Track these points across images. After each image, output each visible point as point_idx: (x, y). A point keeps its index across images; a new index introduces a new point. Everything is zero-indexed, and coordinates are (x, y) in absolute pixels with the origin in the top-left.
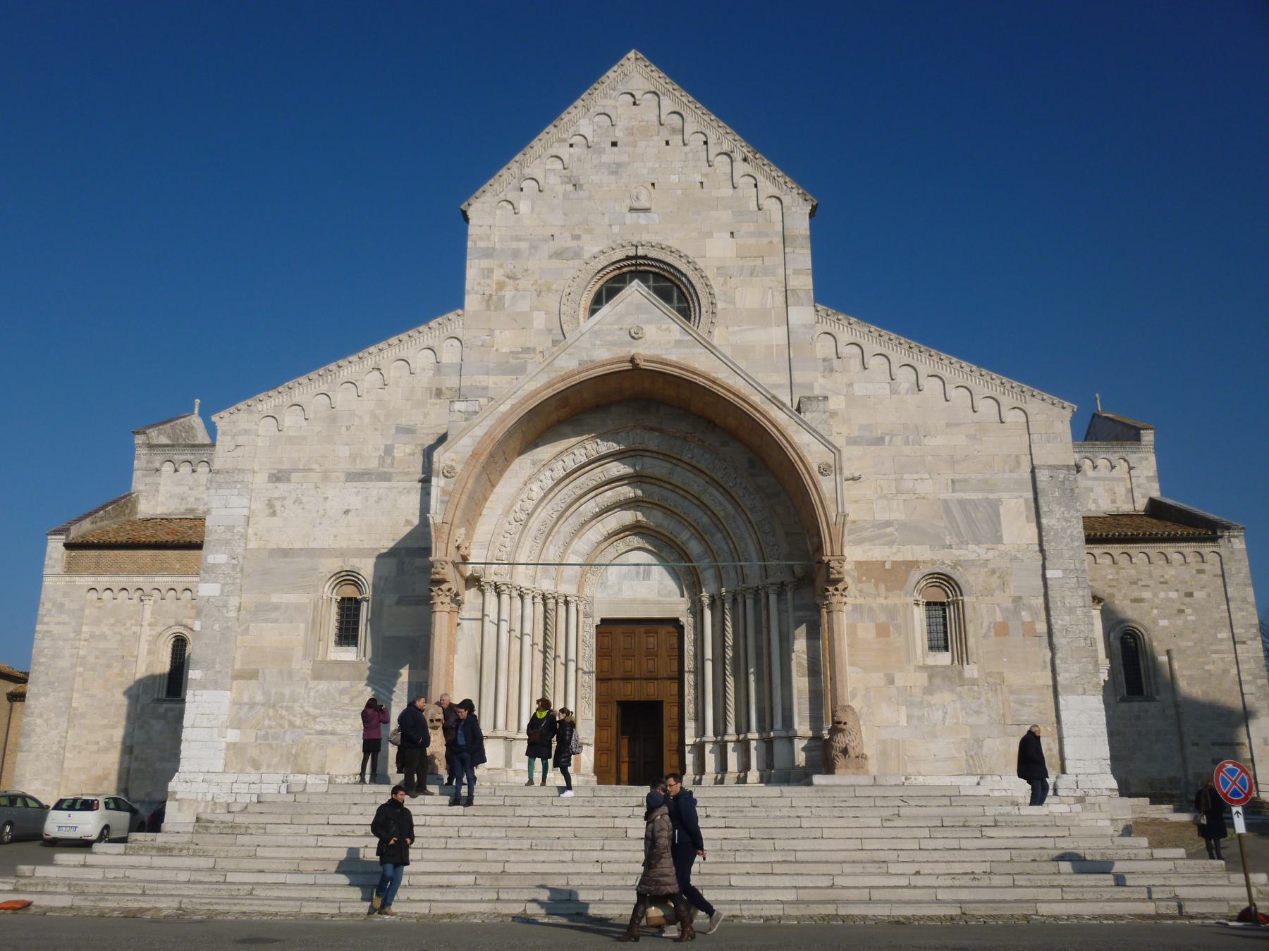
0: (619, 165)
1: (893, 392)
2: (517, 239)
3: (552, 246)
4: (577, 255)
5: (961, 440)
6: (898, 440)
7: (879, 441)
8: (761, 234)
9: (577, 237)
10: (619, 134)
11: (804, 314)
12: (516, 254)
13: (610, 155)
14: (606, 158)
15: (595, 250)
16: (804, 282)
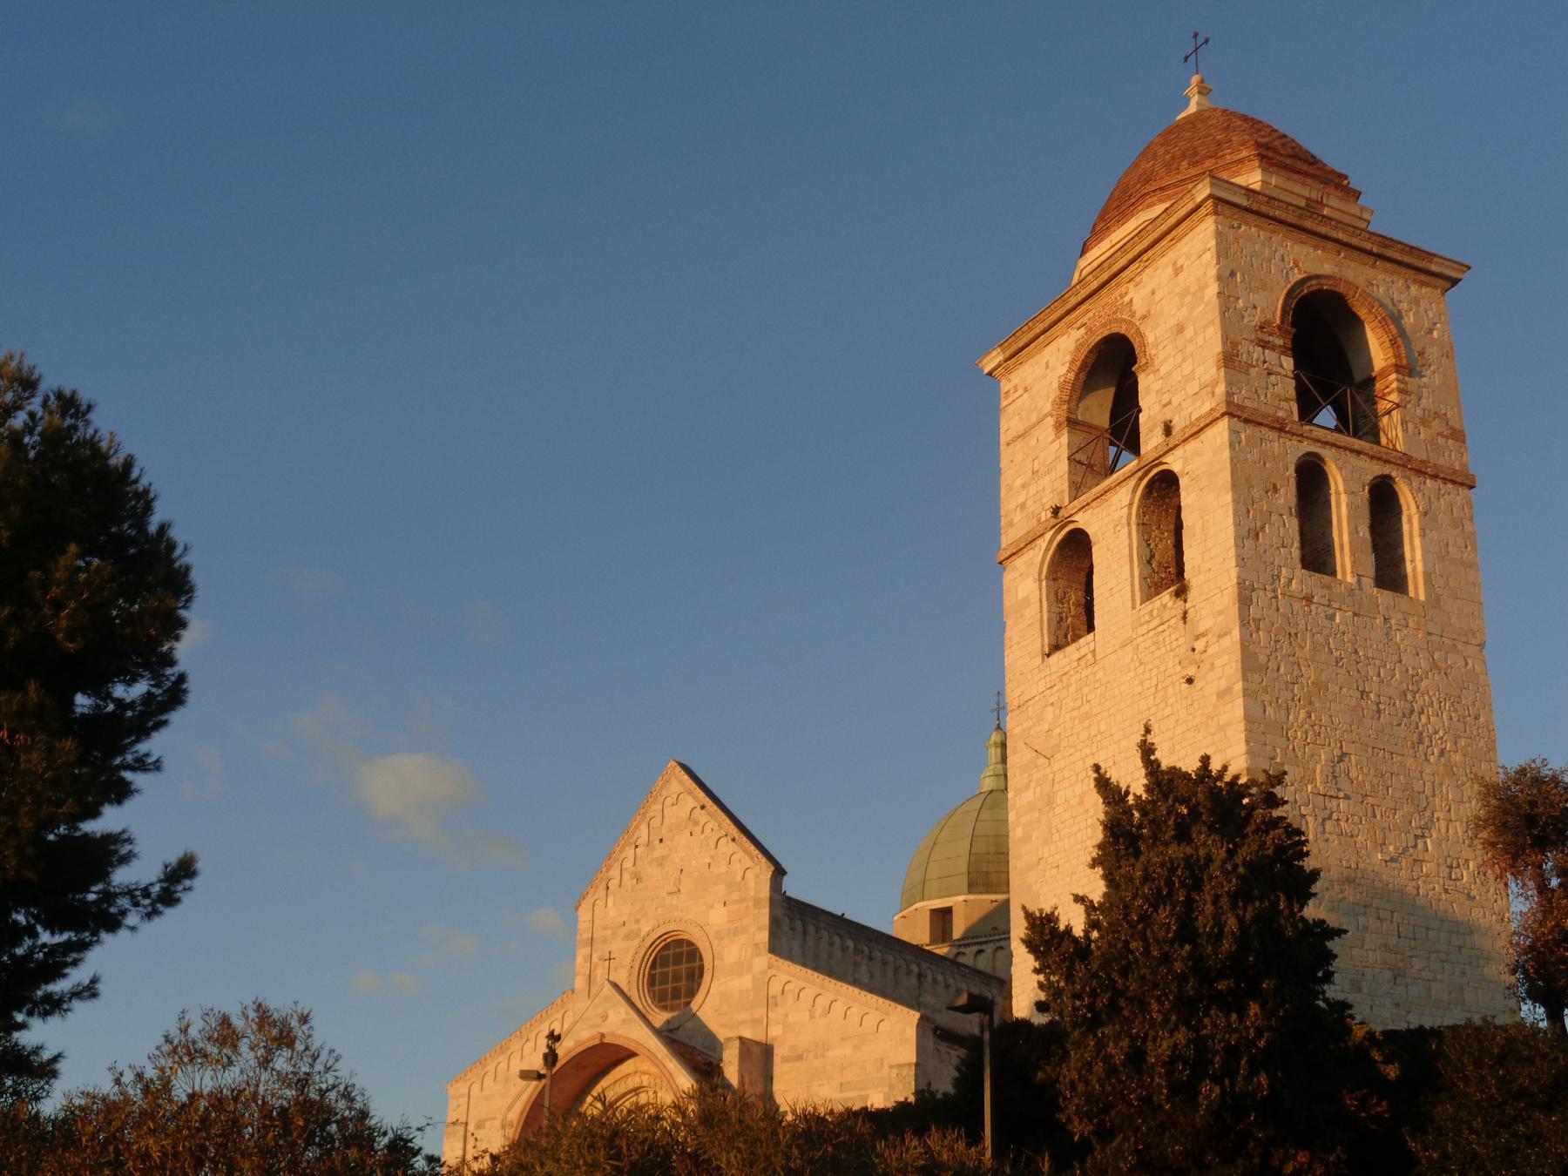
0: (663, 858)
1: (812, 1017)
2: (605, 928)
3: (622, 932)
4: (638, 935)
5: (848, 1050)
6: (811, 1055)
7: (800, 1058)
8: (742, 900)
9: (638, 921)
10: (664, 833)
11: (764, 960)
12: (604, 940)
13: (660, 850)
14: (657, 854)
15: (645, 929)
16: (764, 936)
